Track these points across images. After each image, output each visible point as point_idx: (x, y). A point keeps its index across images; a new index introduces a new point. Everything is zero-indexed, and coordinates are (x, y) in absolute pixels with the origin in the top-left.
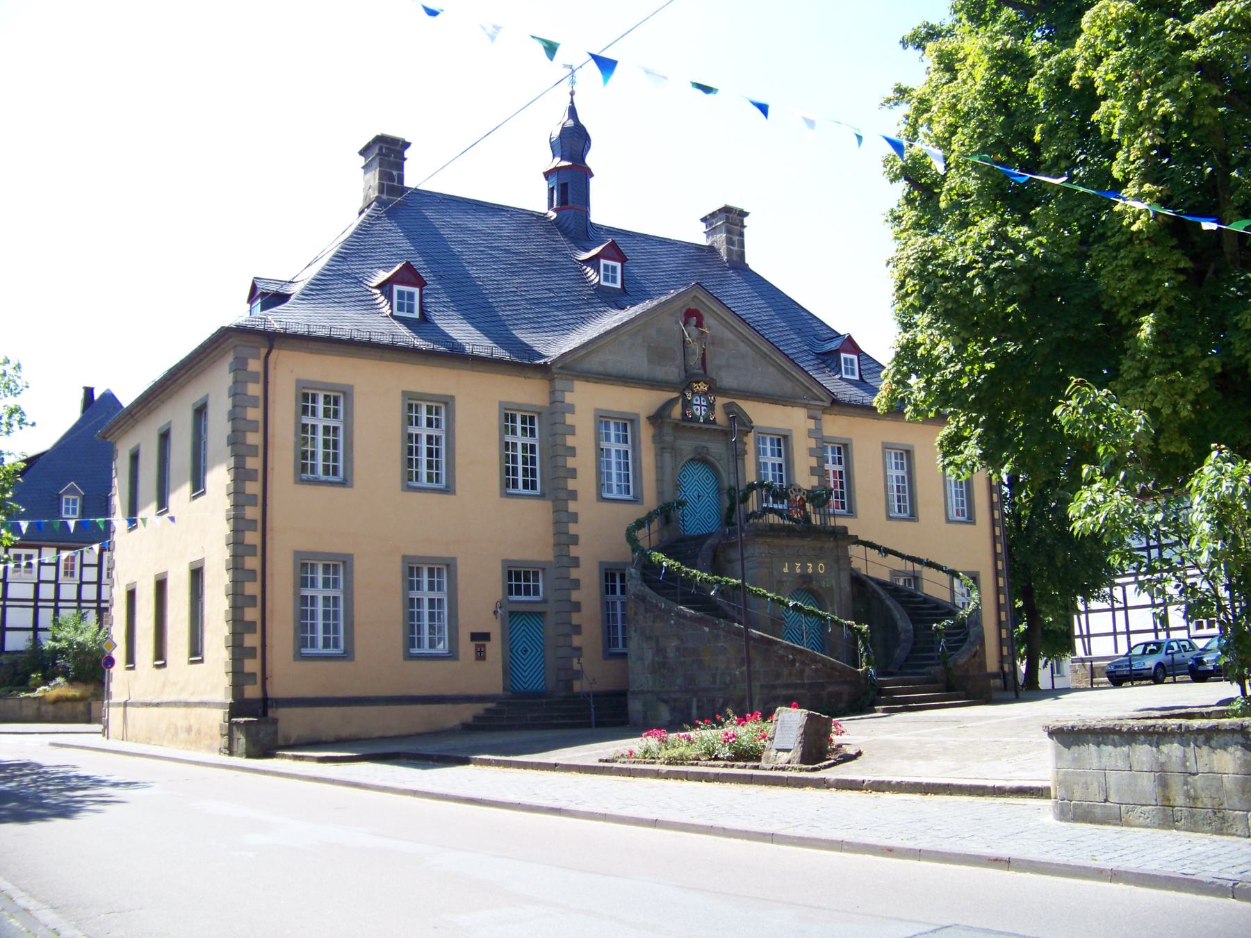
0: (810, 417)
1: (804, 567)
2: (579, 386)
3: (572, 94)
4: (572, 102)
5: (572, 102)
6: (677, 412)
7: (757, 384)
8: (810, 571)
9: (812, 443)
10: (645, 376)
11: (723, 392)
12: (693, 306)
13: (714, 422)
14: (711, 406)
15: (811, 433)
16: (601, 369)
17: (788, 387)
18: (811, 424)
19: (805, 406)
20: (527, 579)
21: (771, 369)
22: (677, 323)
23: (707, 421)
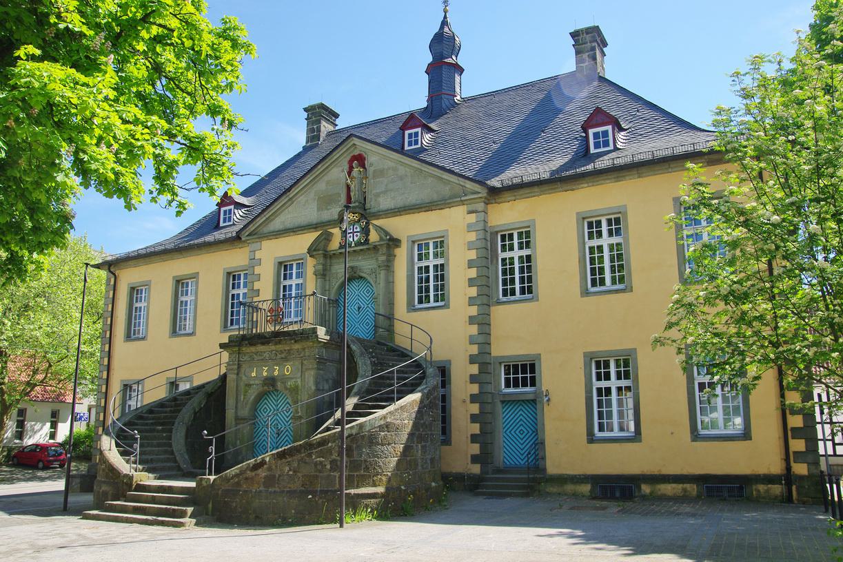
0: (470, 212)
1: (271, 370)
2: (266, 244)
3: (445, 12)
4: (445, 17)
5: (445, 17)
6: (335, 244)
7: (413, 198)
8: (276, 373)
9: (472, 237)
10: (315, 222)
11: (378, 215)
12: (356, 153)
13: (367, 241)
14: (366, 231)
15: (470, 228)
16: (281, 227)
17: (446, 191)
18: (472, 218)
19: (462, 203)
20: (524, 372)
21: (430, 180)
22: (343, 171)
23: (359, 243)
